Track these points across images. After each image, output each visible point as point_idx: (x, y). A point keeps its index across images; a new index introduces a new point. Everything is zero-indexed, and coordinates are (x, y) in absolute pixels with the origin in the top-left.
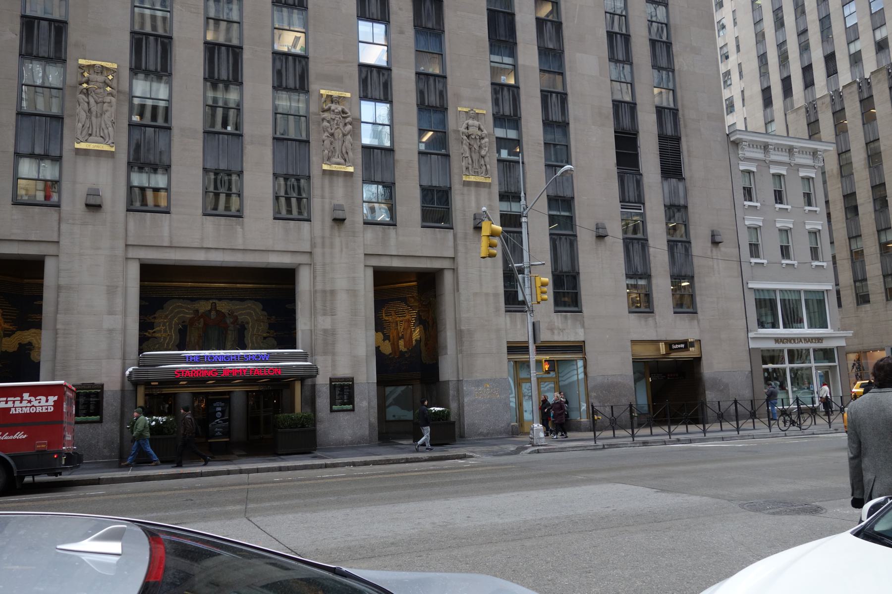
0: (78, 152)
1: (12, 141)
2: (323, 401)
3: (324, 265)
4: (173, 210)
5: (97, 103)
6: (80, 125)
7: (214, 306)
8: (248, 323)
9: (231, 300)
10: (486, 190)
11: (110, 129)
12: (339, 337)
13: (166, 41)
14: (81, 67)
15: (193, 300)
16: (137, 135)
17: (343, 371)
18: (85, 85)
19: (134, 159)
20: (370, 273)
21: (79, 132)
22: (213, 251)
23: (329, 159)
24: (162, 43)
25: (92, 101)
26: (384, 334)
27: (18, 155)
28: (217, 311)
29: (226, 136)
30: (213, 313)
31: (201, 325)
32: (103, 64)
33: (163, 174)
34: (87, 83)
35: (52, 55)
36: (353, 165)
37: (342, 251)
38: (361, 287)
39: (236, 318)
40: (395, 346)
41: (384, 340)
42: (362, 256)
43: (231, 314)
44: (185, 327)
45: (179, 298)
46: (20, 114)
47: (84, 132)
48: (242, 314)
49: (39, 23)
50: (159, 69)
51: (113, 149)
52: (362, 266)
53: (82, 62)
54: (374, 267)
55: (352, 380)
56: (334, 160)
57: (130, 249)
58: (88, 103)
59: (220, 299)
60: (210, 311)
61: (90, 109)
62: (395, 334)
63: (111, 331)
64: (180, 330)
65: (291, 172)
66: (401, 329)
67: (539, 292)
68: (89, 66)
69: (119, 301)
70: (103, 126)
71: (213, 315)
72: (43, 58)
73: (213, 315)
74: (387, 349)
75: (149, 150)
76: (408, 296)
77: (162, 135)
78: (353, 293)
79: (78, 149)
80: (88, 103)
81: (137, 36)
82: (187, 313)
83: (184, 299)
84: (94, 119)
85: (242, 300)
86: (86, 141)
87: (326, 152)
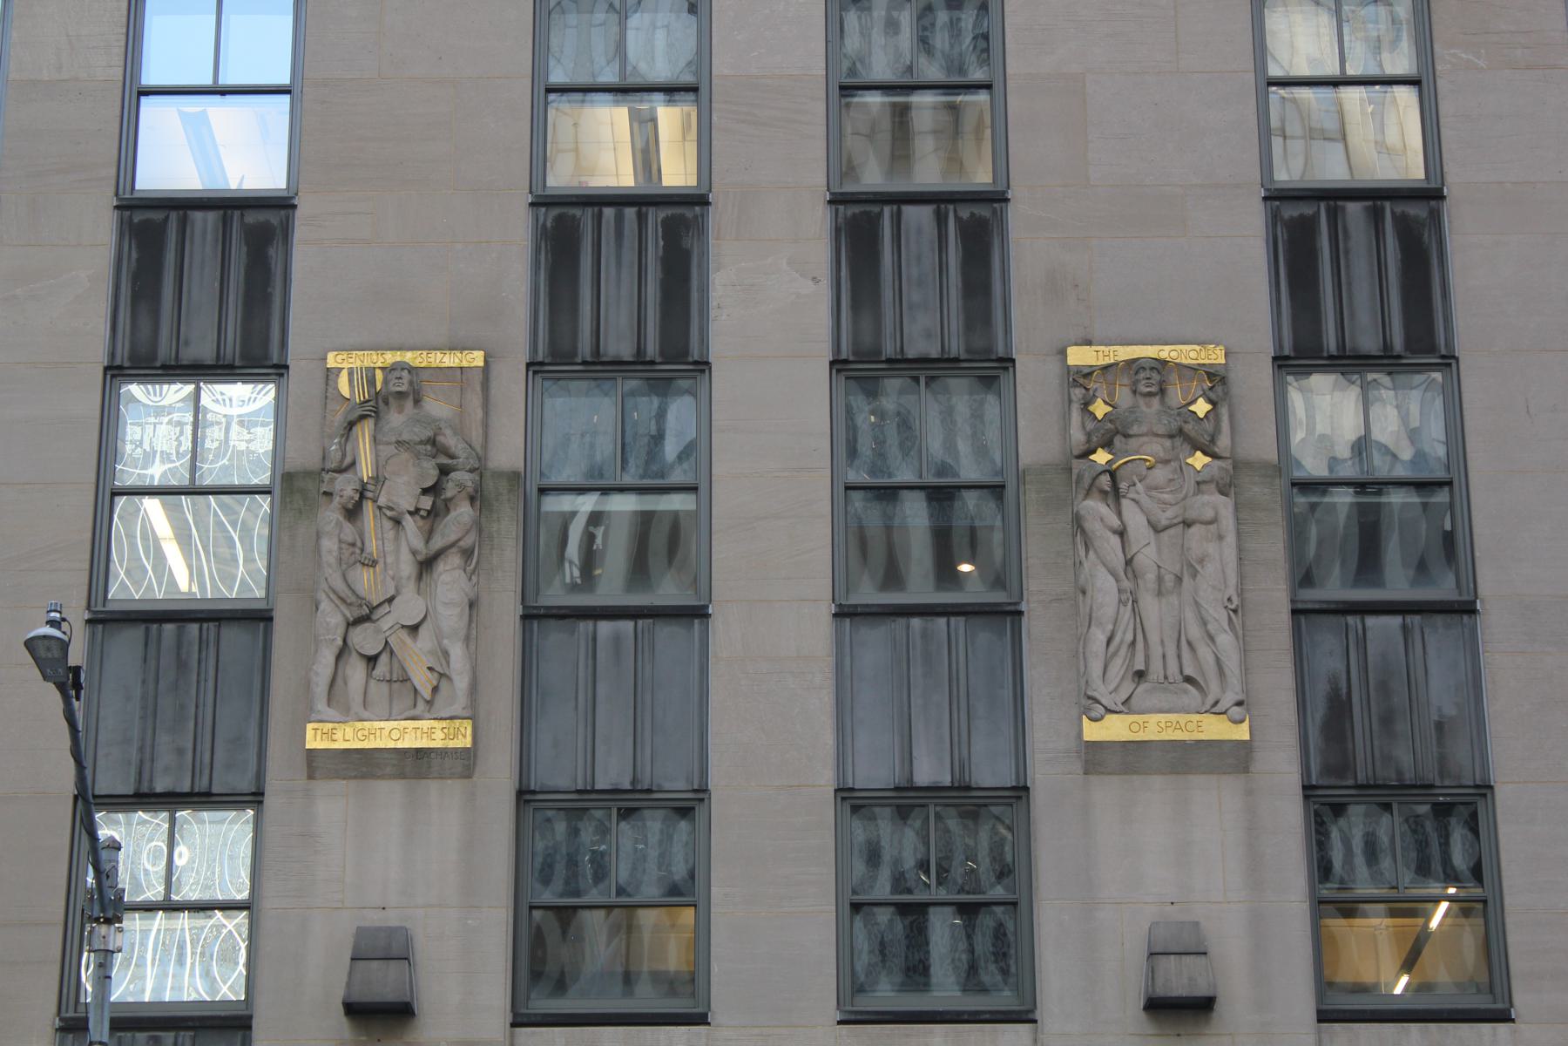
0: (1096, 757)
1: (829, 738)
4: (1523, 1000)
5: (1157, 529)
6: (1099, 637)
11: (1225, 640)
13: (1416, 210)
14: (1081, 377)
16: (1328, 654)
18: (1101, 457)
19: (1327, 770)
21: (1096, 668)
24: (1402, 223)
25: (1135, 521)
32: (1165, 352)
34: (1108, 445)
35: (956, 347)
47: (1117, 667)
49: (897, 220)
50: (1398, 343)
51: (1242, 733)
53: (1079, 356)
58: (1122, 533)
68: (1130, 363)
70: (1194, 631)
72: (924, 361)
75: (1387, 720)
77: (1438, 638)
80: (1122, 533)
81: (1290, 211)
86: (1127, 706)
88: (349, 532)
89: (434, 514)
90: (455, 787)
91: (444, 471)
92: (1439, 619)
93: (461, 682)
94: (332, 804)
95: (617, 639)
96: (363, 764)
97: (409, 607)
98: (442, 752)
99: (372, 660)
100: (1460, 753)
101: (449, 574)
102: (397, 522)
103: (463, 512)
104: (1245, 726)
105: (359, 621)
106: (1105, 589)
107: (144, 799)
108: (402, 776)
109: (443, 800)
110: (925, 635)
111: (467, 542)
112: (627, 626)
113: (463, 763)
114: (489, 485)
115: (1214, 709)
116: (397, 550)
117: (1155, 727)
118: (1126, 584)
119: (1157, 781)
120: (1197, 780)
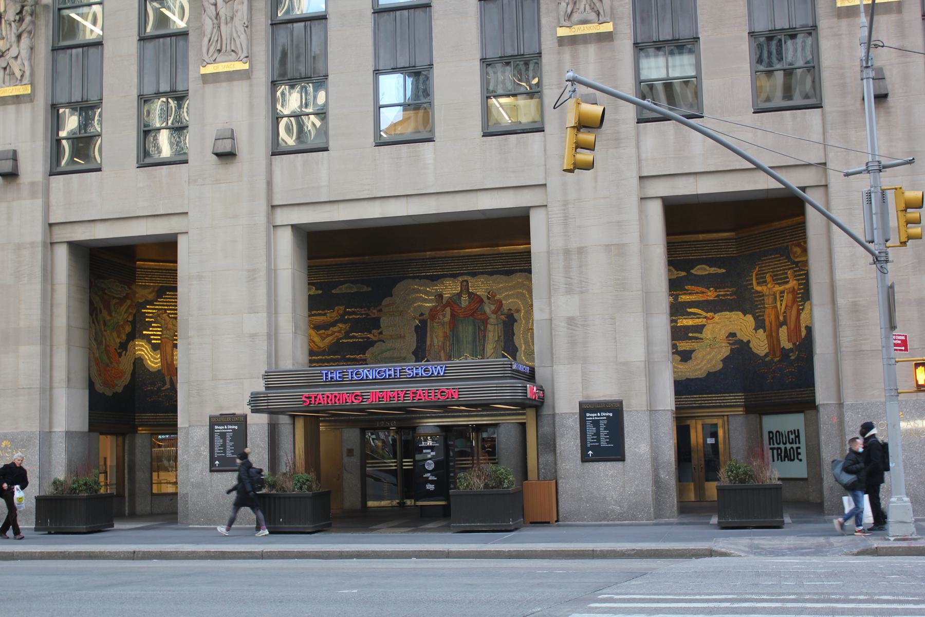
0: (206, 79)
1: (135, 80)
2: (569, 443)
3: (565, 204)
4: (331, 145)
6: (206, 40)
7: (465, 287)
8: (518, 311)
9: (491, 274)
10: (893, 17)
11: (243, 37)
12: (603, 330)
15: (434, 279)
17: (603, 392)
20: (656, 211)
21: (205, 50)
22: (392, 201)
23: (570, 16)
26: (756, 318)
28: (470, 294)
29: (405, 12)
30: (465, 297)
31: (447, 318)
33: (656, 56)
36: (613, 18)
38: (632, 237)
39: (500, 304)
40: (773, 339)
41: (756, 329)
42: (635, 181)
43: (491, 297)
44: (424, 323)
45: (414, 278)
46: (143, 39)
47: (212, 49)
48: (508, 297)
51: (246, 66)
52: (634, 199)
54: (664, 199)
55: (621, 403)
56: (576, 17)
57: (279, 212)
59: (474, 275)
60: (459, 295)
61: (217, 14)
62: (773, 317)
63: (253, 336)
64: (417, 327)
65: (509, 52)
70: (235, 35)
71: (465, 300)
73: (465, 300)
74: (760, 345)
75: (298, 57)
76: (734, 243)
78: (617, 250)
79: (204, 75)
82: (425, 301)
83: (420, 278)
84: (223, 27)
85: (509, 273)
87: (563, 4)
89: (21, 20)
91: (23, 7)
92: (316, 22)
93: (27, 74)
95: (77, 55)
97: (14, 52)
98: (23, 95)
100: (320, 65)
101: (25, 41)
102: (10, 25)
103: (28, 19)
104: (611, 24)
106: (208, 24)
108: (14, 103)
109: (26, 108)
110: (164, 44)
111: (29, 29)
112: (80, 50)
114: (38, 9)
115: (239, 60)
118: (215, 21)
119: (224, 84)
120: (236, 83)
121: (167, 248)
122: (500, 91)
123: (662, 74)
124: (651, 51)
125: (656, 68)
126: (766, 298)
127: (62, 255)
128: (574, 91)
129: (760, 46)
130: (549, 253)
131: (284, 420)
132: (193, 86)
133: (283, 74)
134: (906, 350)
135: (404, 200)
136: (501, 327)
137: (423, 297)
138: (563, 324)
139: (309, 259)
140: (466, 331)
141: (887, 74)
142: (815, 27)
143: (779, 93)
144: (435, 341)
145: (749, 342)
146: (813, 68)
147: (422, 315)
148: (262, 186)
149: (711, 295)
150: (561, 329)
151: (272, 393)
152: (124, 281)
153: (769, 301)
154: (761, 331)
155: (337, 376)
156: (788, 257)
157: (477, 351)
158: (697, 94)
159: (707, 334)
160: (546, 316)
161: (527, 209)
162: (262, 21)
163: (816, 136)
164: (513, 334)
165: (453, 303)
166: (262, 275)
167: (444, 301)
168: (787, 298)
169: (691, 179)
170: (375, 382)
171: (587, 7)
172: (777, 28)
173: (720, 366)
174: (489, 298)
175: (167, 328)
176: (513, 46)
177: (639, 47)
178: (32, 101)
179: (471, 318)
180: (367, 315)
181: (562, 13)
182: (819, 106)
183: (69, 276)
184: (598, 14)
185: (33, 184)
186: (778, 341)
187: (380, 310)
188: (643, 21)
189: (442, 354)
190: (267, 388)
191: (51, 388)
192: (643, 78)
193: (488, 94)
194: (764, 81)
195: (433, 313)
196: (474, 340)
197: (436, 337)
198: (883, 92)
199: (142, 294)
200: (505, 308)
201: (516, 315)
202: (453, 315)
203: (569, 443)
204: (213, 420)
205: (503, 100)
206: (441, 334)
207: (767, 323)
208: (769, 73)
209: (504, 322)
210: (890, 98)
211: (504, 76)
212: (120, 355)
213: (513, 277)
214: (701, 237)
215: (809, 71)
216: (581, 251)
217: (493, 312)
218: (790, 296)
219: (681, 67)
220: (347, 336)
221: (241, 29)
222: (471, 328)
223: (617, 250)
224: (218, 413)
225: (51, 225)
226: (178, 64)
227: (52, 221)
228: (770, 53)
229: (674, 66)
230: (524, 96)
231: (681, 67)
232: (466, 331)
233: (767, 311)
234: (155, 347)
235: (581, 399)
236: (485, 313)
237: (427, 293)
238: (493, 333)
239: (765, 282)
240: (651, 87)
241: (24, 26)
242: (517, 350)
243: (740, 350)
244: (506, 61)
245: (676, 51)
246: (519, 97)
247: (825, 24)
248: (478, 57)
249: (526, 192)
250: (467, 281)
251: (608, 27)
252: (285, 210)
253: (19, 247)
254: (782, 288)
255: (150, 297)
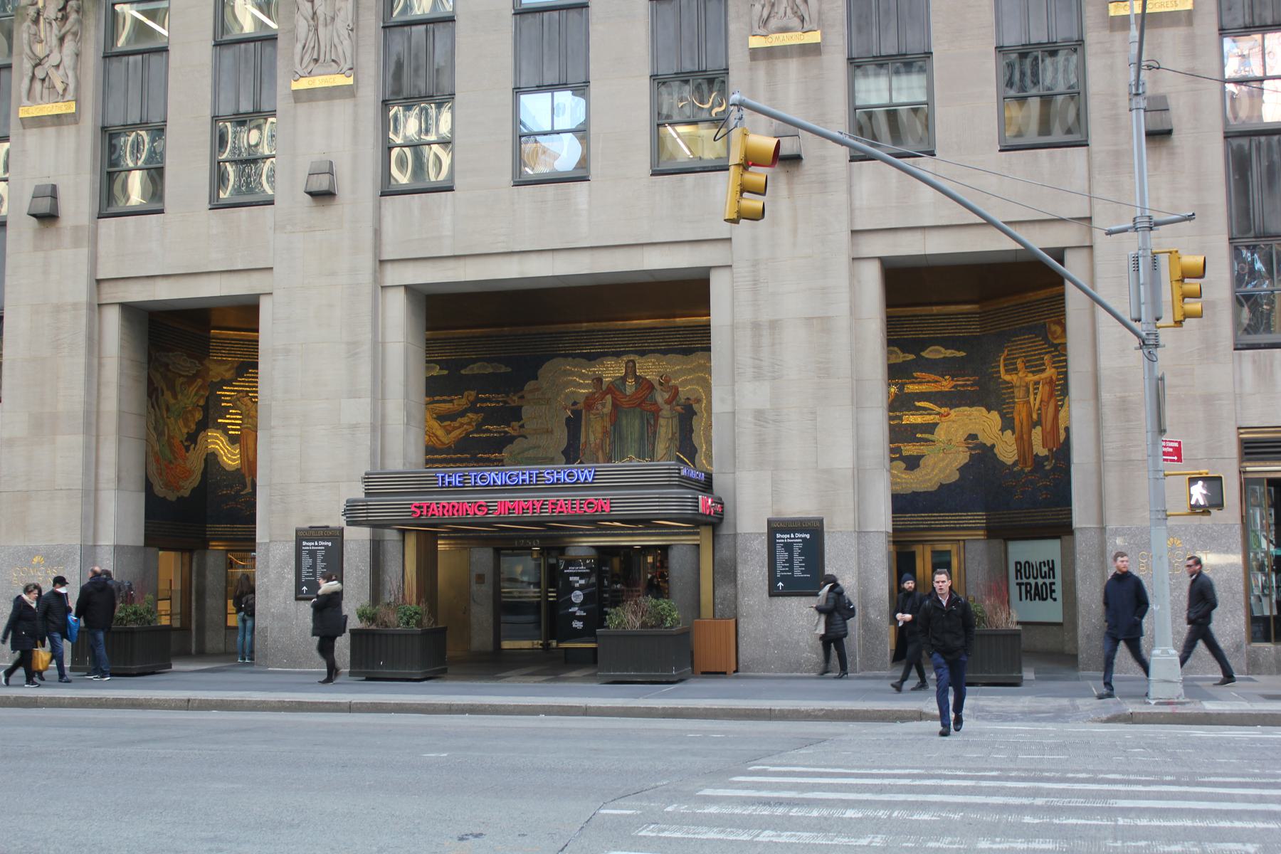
0: (298, 96)
1: (209, 96)
3: (755, 264)
6: (299, 46)
8: (699, 401)
9: (665, 352)
11: (347, 43)
12: (802, 430)
15: (591, 358)
17: (798, 506)
19: (394, 93)
20: (872, 278)
21: (297, 59)
22: (533, 256)
26: (1003, 416)
27: (518, 91)
28: (637, 378)
29: (556, 14)
30: (630, 382)
31: (608, 409)
36: (821, 24)
37: (795, 231)
38: (840, 308)
39: (675, 392)
40: (1024, 443)
41: (1003, 430)
42: (845, 235)
43: (665, 382)
44: (577, 414)
45: (566, 356)
48: (685, 383)
51: (350, 81)
52: (844, 260)
54: (883, 261)
55: (821, 521)
56: (773, 23)
57: (389, 268)
59: (642, 353)
60: (624, 379)
61: (315, 13)
62: (1024, 414)
63: (354, 427)
64: (568, 419)
65: (688, 67)
66: (1035, 402)
67: (1167, 292)
69: (365, 369)
70: (336, 40)
74: (1007, 451)
75: (417, 70)
76: (973, 318)
78: (820, 324)
79: (295, 92)
82: (580, 386)
83: (574, 356)
84: (321, 29)
87: (758, 7)
88: (33, 28)
89: (65, 18)
90: (73, 128)
93: (71, 87)
94: (32, 136)
95: (136, 63)
96: (39, 122)
97: (54, 59)
98: (66, 115)
99: (43, 80)
100: (445, 82)
101: (69, 45)
102: (50, 24)
105: (37, 65)
106: (302, 26)
107: (540, 88)
108: (54, 125)
109: (69, 131)
110: (246, 50)
111: (74, 29)
112: (140, 57)
113: (74, 119)
116: (49, 33)
117: (319, 82)
118: (311, 22)
119: (321, 103)
120: (337, 102)
121: (245, 313)
122: (676, 118)
123: (884, 99)
124: (871, 68)
125: (876, 91)
126: (1016, 390)
127: (113, 320)
128: (741, 119)
129: (1010, 66)
130: (734, 327)
131: (391, 535)
132: (282, 104)
133: (397, 91)
134: (1180, 460)
135: (549, 256)
136: (676, 421)
137: (577, 380)
138: (750, 419)
139: (428, 329)
140: (632, 426)
141: (1172, 103)
142: (1081, 42)
143: (1034, 126)
144: (592, 438)
145: (993, 446)
146: (1077, 95)
147: (575, 404)
148: (368, 235)
149: (946, 384)
150: (747, 425)
151: (374, 501)
152: (191, 353)
153: (1019, 393)
154: (1009, 432)
155: (456, 480)
156: (1045, 339)
157: (646, 452)
158: (928, 125)
159: (940, 434)
160: (728, 408)
161: (708, 270)
162: (371, 23)
163: (1080, 183)
164: (692, 431)
165: (615, 389)
166: (366, 348)
167: (604, 387)
168: (1043, 390)
169: (918, 235)
170: (504, 489)
171: (789, 11)
172: (1033, 41)
173: (956, 476)
174: (661, 384)
175: (249, 416)
176: (692, 59)
177: (855, 64)
178: (76, 123)
179: (638, 409)
180: (505, 402)
181: (756, 18)
182: (1084, 144)
183: (122, 347)
184: (803, 20)
185: (76, 228)
186: (1031, 445)
187: (522, 397)
188: (860, 30)
189: (600, 454)
190: (367, 494)
191: (96, 490)
192: (858, 103)
193: (660, 120)
194: (1014, 111)
195: (590, 402)
196: (641, 438)
197: (593, 433)
198: (1167, 127)
199: (217, 371)
200: (682, 397)
201: (695, 407)
202: (615, 405)
203: (753, 572)
204: (300, 534)
205: (682, 129)
206: (599, 429)
207: (1017, 422)
208: (1022, 100)
209: (680, 414)
210: (1175, 136)
211: (678, 99)
212: (187, 449)
213: (692, 357)
214: (935, 309)
215: (1072, 98)
216: (774, 325)
217: (669, 402)
218: (1047, 388)
219: (907, 90)
220: (479, 429)
221: (344, 33)
222: (637, 423)
223: (820, 324)
224: (306, 525)
225: (99, 281)
226: (262, 77)
227: (99, 277)
228: (1023, 74)
229: (899, 89)
230: (706, 124)
231: (907, 90)
232: (632, 426)
233: (1017, 406)
234: (233, 440)
235: (770, 516)
236: (656, 403)
237: (582, 376)
238: (666, 429)
239: (1016, 369)
240: (870, 116)
241: (68, 26)
242: (696, 451)
243: (982, 456)
244: (684, 78)
245: (902, 69)
246: (701, 125)
247: (1091, 38)
248: (648, 72)
249: (705, 248)
250: (633, 361)
251: (814, 37)
252: (396, 265)
253: (58, 309)
254: (1036, 378)
255: (228, 375)
